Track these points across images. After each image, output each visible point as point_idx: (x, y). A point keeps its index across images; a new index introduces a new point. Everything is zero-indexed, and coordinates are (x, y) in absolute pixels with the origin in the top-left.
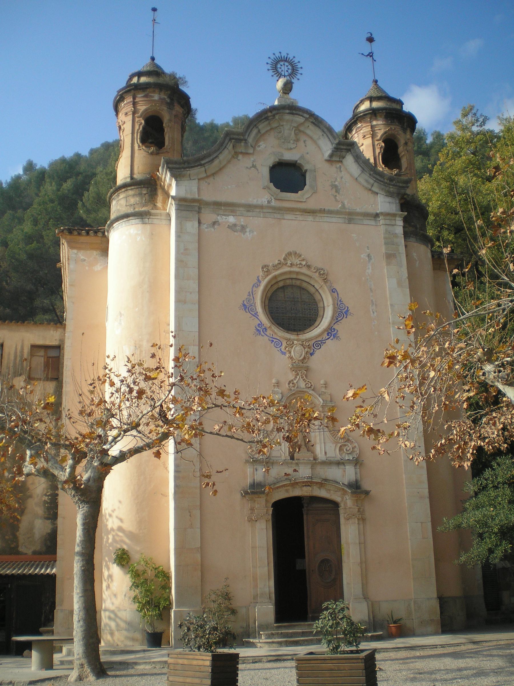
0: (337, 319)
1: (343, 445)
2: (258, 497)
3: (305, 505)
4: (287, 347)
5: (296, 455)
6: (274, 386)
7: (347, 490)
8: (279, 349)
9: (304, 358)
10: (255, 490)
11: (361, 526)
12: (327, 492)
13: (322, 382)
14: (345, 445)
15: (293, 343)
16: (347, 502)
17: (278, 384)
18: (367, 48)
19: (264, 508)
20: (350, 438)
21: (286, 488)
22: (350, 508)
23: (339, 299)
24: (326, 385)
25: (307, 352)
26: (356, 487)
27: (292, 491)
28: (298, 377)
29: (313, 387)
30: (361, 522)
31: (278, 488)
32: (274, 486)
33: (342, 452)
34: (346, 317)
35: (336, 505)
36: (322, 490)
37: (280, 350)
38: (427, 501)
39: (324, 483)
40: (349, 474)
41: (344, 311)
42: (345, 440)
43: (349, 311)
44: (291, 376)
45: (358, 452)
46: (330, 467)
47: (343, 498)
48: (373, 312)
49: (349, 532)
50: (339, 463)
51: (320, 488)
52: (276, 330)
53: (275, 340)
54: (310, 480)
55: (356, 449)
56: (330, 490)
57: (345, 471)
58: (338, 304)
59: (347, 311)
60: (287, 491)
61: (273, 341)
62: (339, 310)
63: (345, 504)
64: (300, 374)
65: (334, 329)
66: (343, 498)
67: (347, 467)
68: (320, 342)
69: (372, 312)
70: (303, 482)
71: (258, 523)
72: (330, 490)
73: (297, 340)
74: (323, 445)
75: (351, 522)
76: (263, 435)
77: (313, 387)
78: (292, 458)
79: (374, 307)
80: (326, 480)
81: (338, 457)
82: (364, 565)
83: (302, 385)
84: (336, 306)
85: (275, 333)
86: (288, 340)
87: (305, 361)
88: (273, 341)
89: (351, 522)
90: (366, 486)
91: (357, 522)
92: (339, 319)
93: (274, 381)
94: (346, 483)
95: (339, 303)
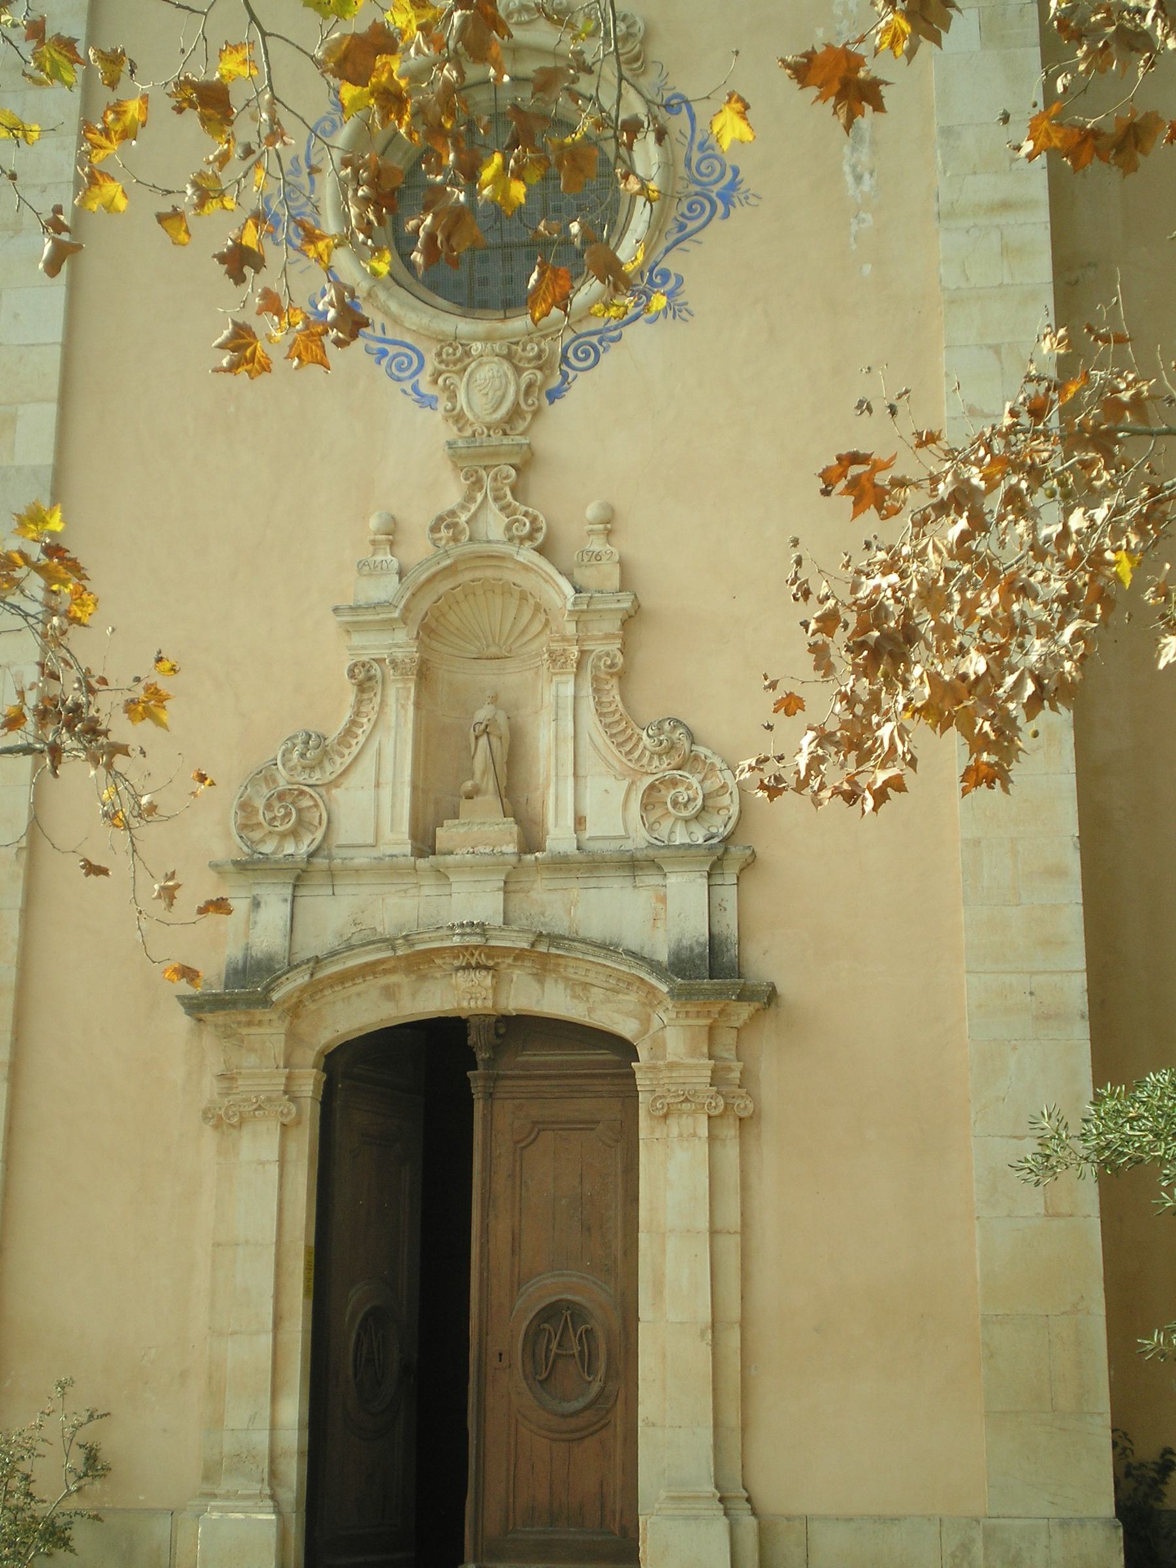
0: (682, 227)
1: (662, 781)
2: (249, 1024)
3: (482, 1056)
4: (440, 374)
5: (445, 835)
6: (374, 542)
7: (653, 981)
8: (407, 386)
9: (516, 413)
10: (242, 993)
11: (731, 1153)
12: (574, 996)
13: (591, 511)
14: (674, 783)
15: (467, 353)
16: (668, 1042)
17: (392, 533)
18: (901, 406)
19: (279, 1069)
20: (701, 750)
21: (384, 981)
22: (671, 1066)
23: (698, 138)
24: (609, 524)
25: (530, 386)
26: (712, 973)
27: (414, 995)
28: (479, 497)
29: (540, 537)
30: (730, 1132)
31: (344, 978)
32: (326, 976)
33: (658, 812)
34: (726, 215)
35: (625, 1049)
36: (549, 983)
37: (415, 388)
38: (1081, 1033)
39: (547, 951)
40: (678, 910)
41: (716, 188)
42: (676, 760)
43: (743, 187)
44: (452, 494)
45: (734, 810)
46: (593, 882)
47: (646, 1022)
48: (858, 178)
49: (673, 1173)
50: (633, 865)
51: (540, 978)
52: (393, 306)
53: (392, 350)
54: (476, 940)
55: (725, 800)
56: (586, 986)
57: (663, 899)
58: (688, 163)
59: (733, 186)
60: (389, 993)
61: (384, 353)
62: (698, 189)
63: (658, 1046)
64: (488, 483)
65: (666, 275)
66: (646, 1022)
67: (672, 880)
68: (594, 340)
69: (849, 179)
70: (455, 951)
71: (246, 1133)
72: (586, 986)
73: (488, 338)
74: (586, 791)
75: (675, 1131)
76: (302, 755)
77: (540, 537)
78: (424, 843)
79: (864, 155)
80: (555, 939)
81: (639, 839)
82: (735, 1333)
83: (494, 524)
84: (682, 171)
85: (396, 320)
86: (442, 340)
87: (522, 426)
88: (384, 353)
89: (675, 1131)
90: (768, 961)
91: (704, 1132)
92: (692, 226)
93: (374, 523)
94: (663, 956)
95: (696, 156)
